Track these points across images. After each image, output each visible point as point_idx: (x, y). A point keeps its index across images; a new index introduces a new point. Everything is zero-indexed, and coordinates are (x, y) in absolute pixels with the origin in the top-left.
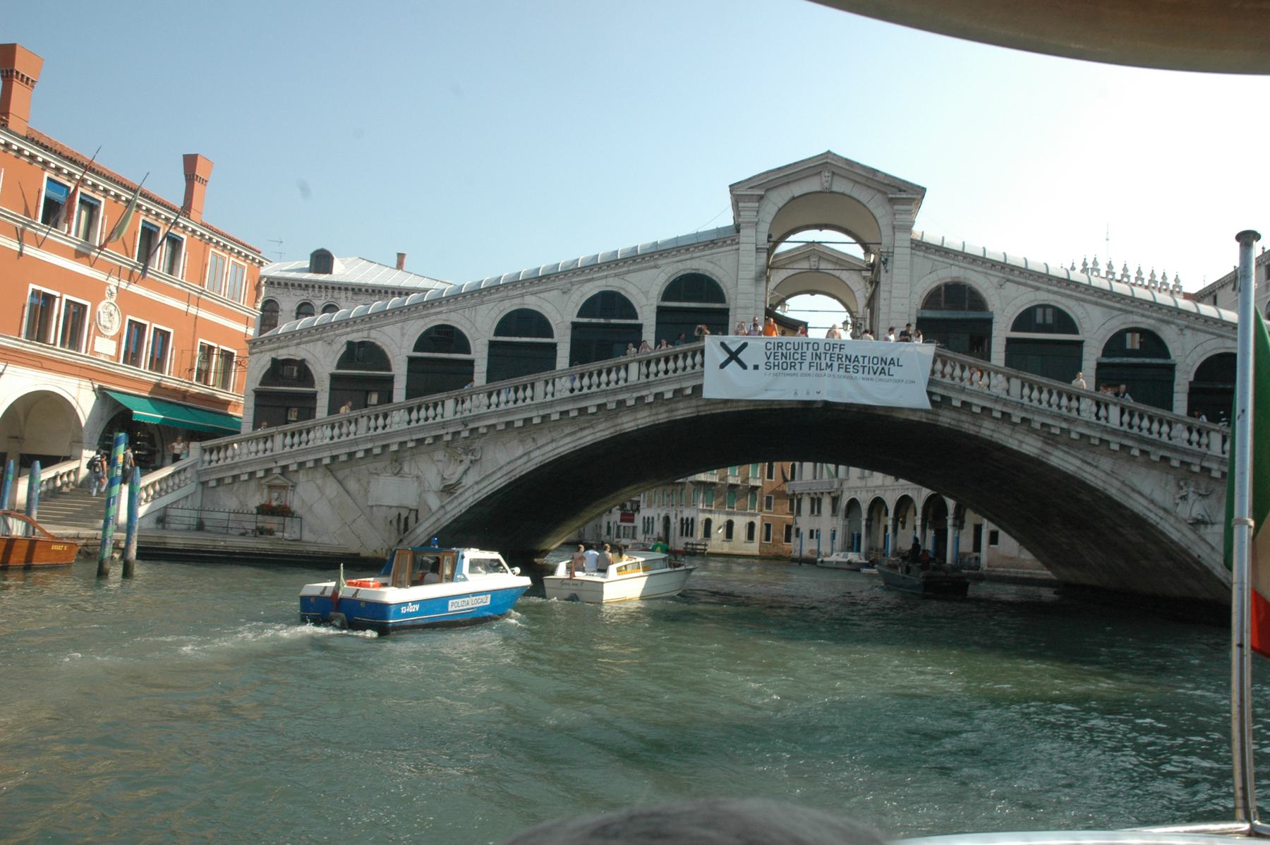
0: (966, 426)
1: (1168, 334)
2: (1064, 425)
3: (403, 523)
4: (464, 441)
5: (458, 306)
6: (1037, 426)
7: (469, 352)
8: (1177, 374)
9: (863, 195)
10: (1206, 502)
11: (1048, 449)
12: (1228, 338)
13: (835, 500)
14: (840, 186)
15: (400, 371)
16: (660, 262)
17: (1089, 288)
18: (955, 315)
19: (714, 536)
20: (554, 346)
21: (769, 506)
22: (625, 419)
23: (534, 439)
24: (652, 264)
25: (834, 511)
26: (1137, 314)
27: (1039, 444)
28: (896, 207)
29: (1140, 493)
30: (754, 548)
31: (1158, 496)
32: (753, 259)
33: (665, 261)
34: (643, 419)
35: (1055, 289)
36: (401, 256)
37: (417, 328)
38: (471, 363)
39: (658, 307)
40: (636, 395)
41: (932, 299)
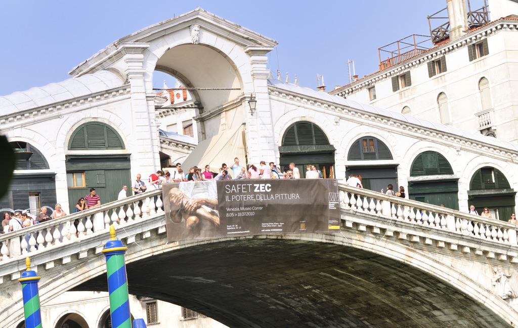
0: (354, 242)
1: (449, 155)
2: (422, 234)
6: (404, 237)
8: (460, 186)
10: (510, 280)
11: (410, 254)
12: (485, 155)
14: (208, 39)
16: (61, 112)
22: (91, 266)
23: (9, 294)
24: (56, 113)
26: (429, 140)
27: (405, 251)
29: (472, 281)
31: (482, 281)
32: (144, 108)
33: (67, 110)
35: (374, 123)
39: (66, 156)
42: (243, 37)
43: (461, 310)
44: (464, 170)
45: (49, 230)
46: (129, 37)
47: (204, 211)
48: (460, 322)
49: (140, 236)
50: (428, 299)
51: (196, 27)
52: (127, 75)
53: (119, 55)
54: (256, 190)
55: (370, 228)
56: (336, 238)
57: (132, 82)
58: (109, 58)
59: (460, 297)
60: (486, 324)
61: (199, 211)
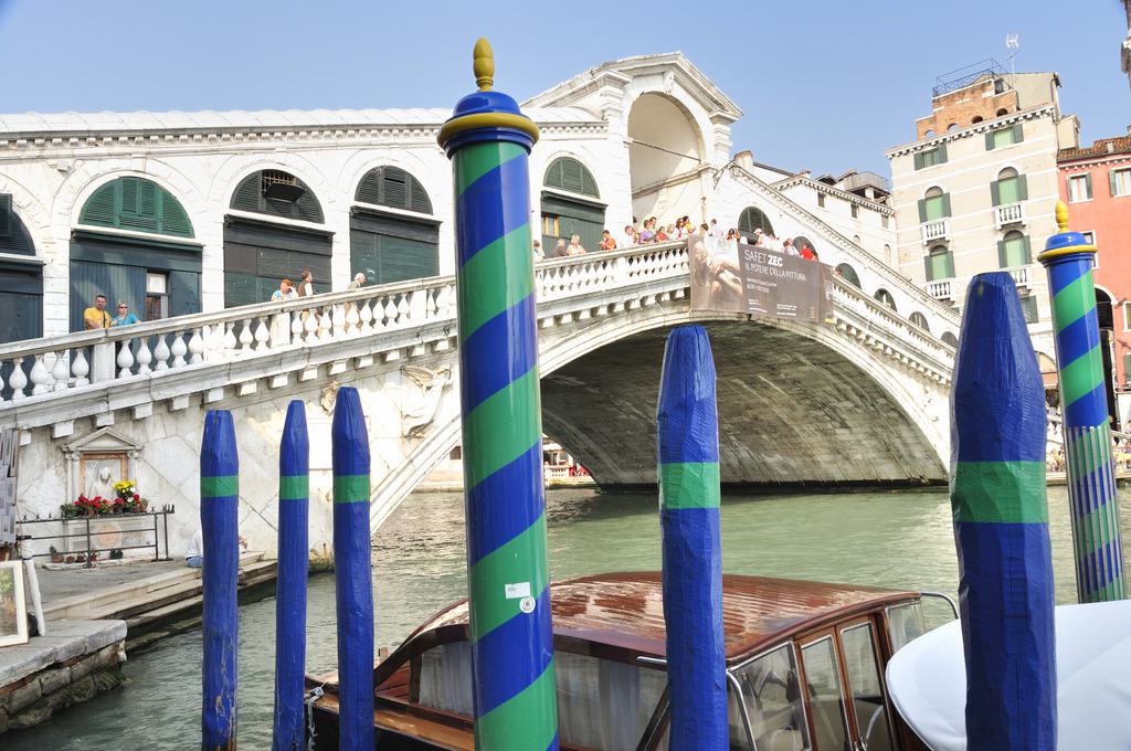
5: (299, 142)
7: (320, 220)
14: (679, 93)
20: (433, 227)
28: (718, 126)
38: (326, 238)
40: (626, 298)
42: (712, 99)
43: (879, 430)
45: (567, 269)
46: (614, 63)
47: (727, 277)
48: (865, 442)
49: (658, 297)
50: (843, 416)
51: (671, 74)
52: (604, 111)
53: (594, 86)
54: (770, 263)
55: (849, 327)
56: (819, 335)
57: (610, 119)
58: (574, 93)
59: (895, 415)
60: (900, 447)
61: (721, 276)
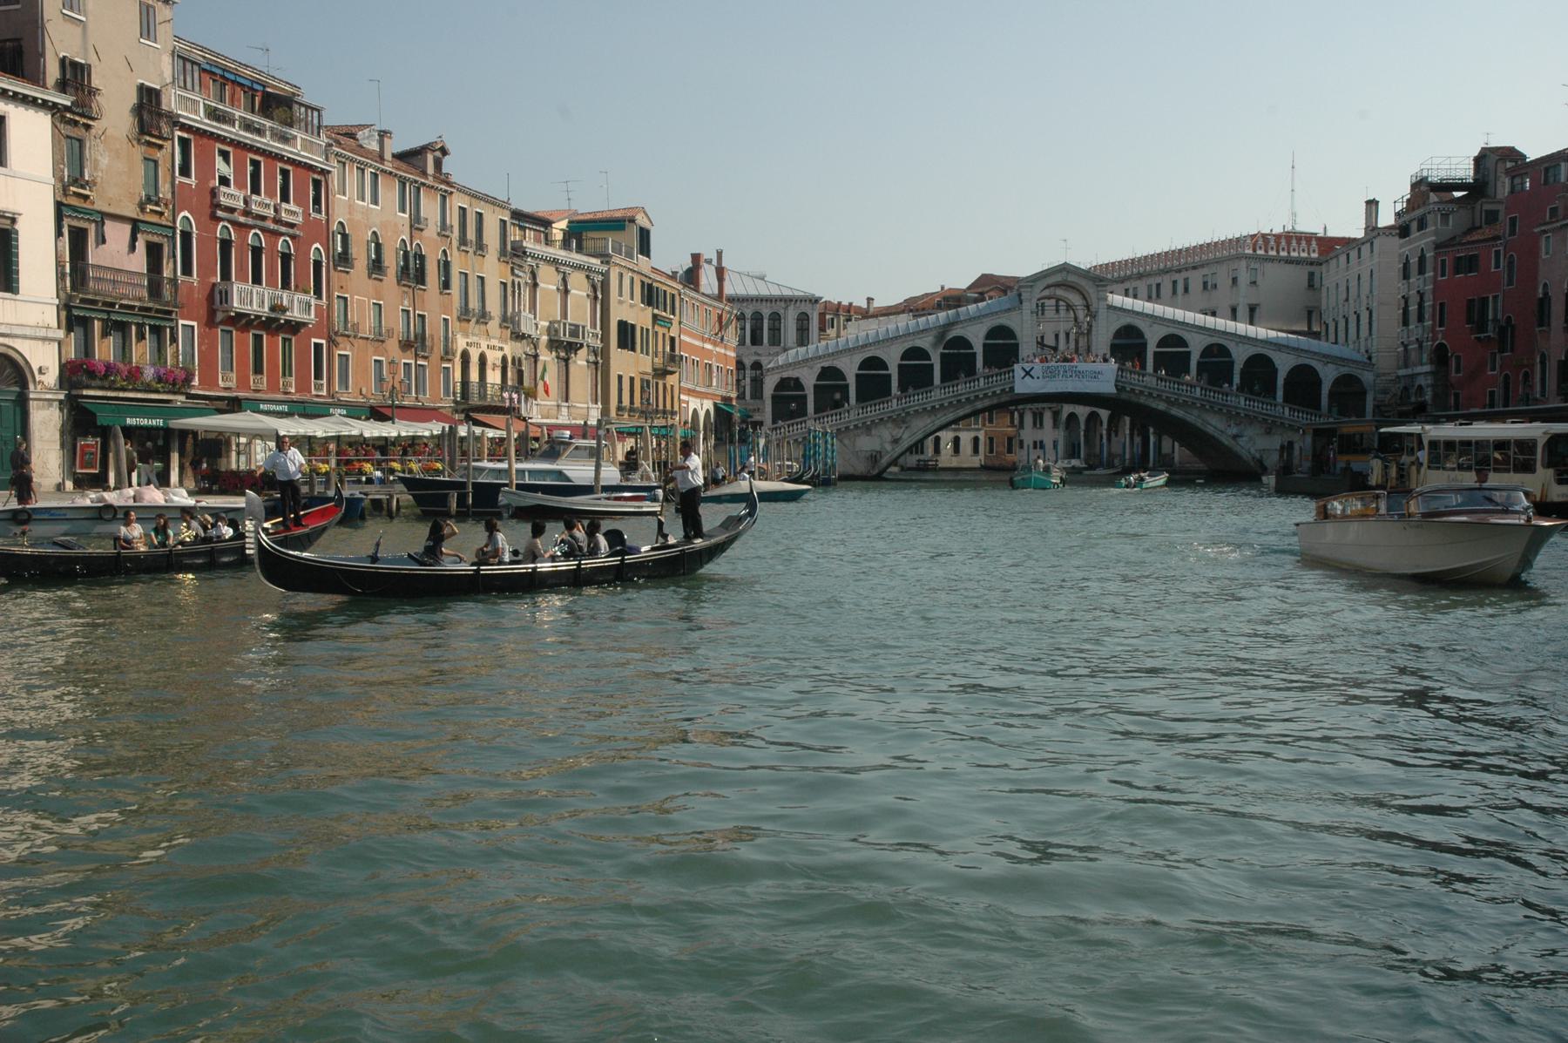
1: (1231, 346)
3: (874, 458)
4: (900, 420)
9: (1083, 283)
13: (1056, 415)
14: (1072, 278)
15: (851, 381)
17: (1193, 326)
18: (1128, 344)
19: (943, 452)
21: (991, 421)
25: (1056, 425)
30: (976, 461)
34: (987, 403)
36: (720, 254)
37: (858, 358)
38: (889, 376)
41: (1119, 333)
44: (1240, 355)
55: (1141, 392)
